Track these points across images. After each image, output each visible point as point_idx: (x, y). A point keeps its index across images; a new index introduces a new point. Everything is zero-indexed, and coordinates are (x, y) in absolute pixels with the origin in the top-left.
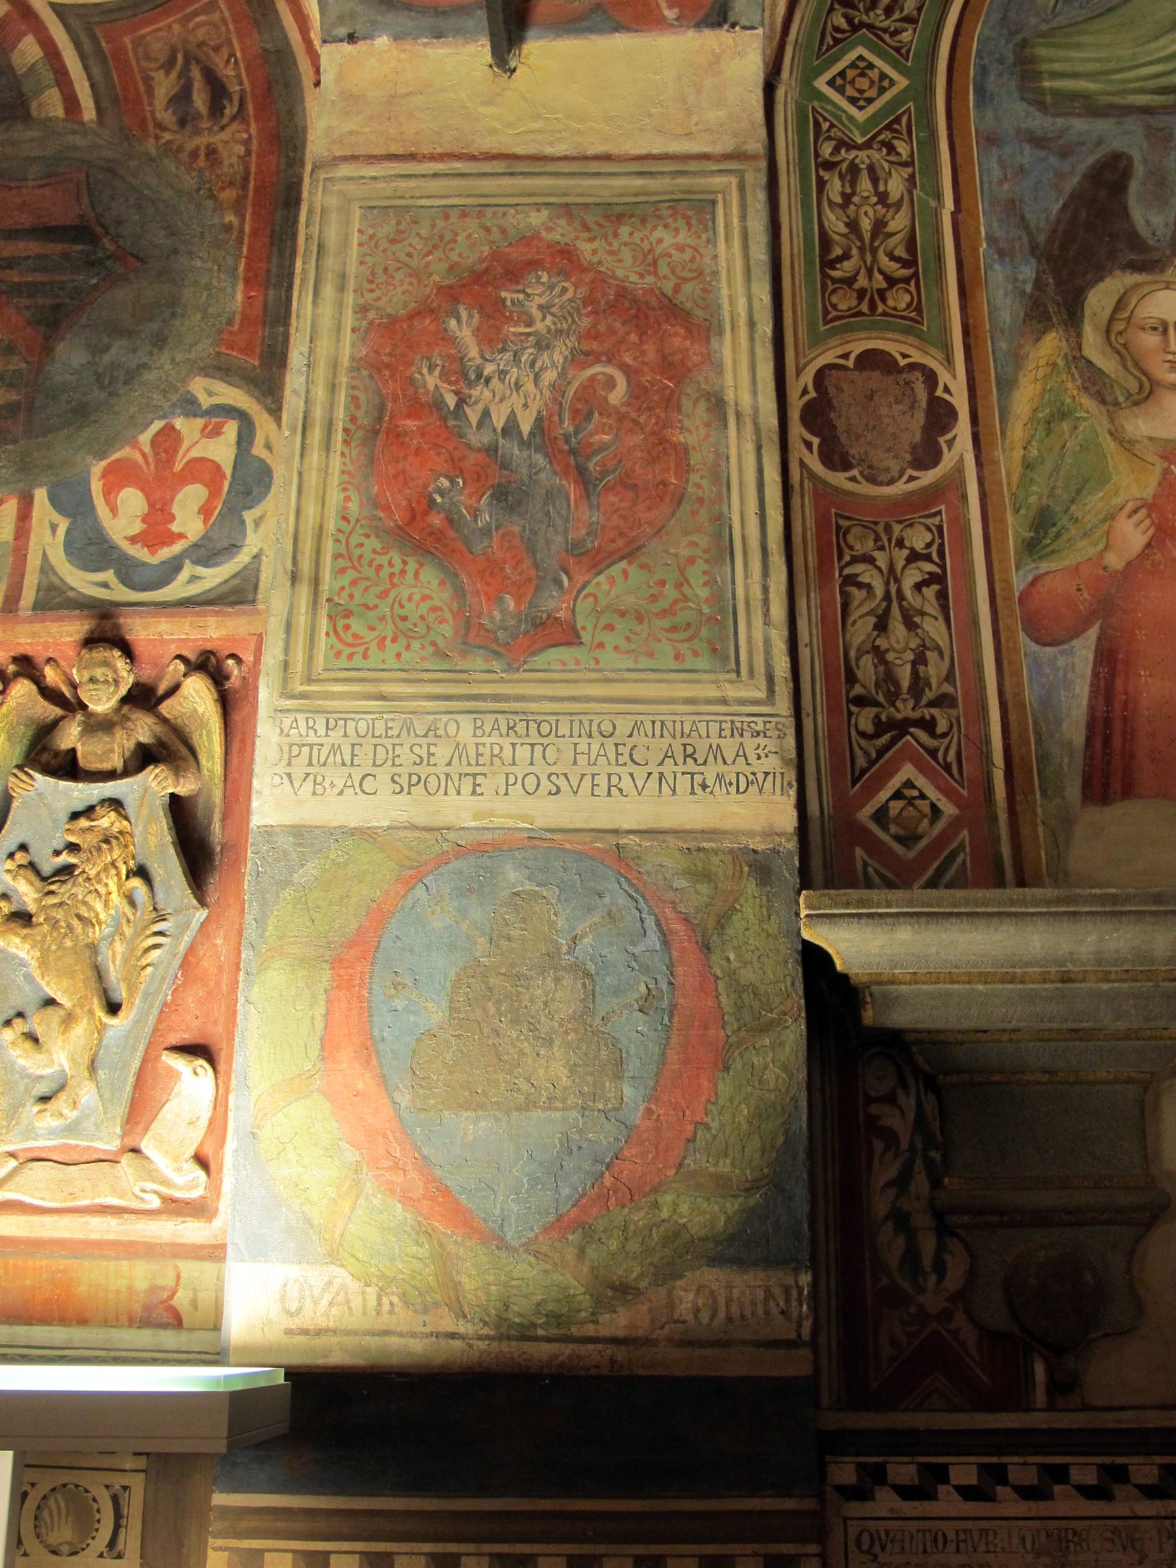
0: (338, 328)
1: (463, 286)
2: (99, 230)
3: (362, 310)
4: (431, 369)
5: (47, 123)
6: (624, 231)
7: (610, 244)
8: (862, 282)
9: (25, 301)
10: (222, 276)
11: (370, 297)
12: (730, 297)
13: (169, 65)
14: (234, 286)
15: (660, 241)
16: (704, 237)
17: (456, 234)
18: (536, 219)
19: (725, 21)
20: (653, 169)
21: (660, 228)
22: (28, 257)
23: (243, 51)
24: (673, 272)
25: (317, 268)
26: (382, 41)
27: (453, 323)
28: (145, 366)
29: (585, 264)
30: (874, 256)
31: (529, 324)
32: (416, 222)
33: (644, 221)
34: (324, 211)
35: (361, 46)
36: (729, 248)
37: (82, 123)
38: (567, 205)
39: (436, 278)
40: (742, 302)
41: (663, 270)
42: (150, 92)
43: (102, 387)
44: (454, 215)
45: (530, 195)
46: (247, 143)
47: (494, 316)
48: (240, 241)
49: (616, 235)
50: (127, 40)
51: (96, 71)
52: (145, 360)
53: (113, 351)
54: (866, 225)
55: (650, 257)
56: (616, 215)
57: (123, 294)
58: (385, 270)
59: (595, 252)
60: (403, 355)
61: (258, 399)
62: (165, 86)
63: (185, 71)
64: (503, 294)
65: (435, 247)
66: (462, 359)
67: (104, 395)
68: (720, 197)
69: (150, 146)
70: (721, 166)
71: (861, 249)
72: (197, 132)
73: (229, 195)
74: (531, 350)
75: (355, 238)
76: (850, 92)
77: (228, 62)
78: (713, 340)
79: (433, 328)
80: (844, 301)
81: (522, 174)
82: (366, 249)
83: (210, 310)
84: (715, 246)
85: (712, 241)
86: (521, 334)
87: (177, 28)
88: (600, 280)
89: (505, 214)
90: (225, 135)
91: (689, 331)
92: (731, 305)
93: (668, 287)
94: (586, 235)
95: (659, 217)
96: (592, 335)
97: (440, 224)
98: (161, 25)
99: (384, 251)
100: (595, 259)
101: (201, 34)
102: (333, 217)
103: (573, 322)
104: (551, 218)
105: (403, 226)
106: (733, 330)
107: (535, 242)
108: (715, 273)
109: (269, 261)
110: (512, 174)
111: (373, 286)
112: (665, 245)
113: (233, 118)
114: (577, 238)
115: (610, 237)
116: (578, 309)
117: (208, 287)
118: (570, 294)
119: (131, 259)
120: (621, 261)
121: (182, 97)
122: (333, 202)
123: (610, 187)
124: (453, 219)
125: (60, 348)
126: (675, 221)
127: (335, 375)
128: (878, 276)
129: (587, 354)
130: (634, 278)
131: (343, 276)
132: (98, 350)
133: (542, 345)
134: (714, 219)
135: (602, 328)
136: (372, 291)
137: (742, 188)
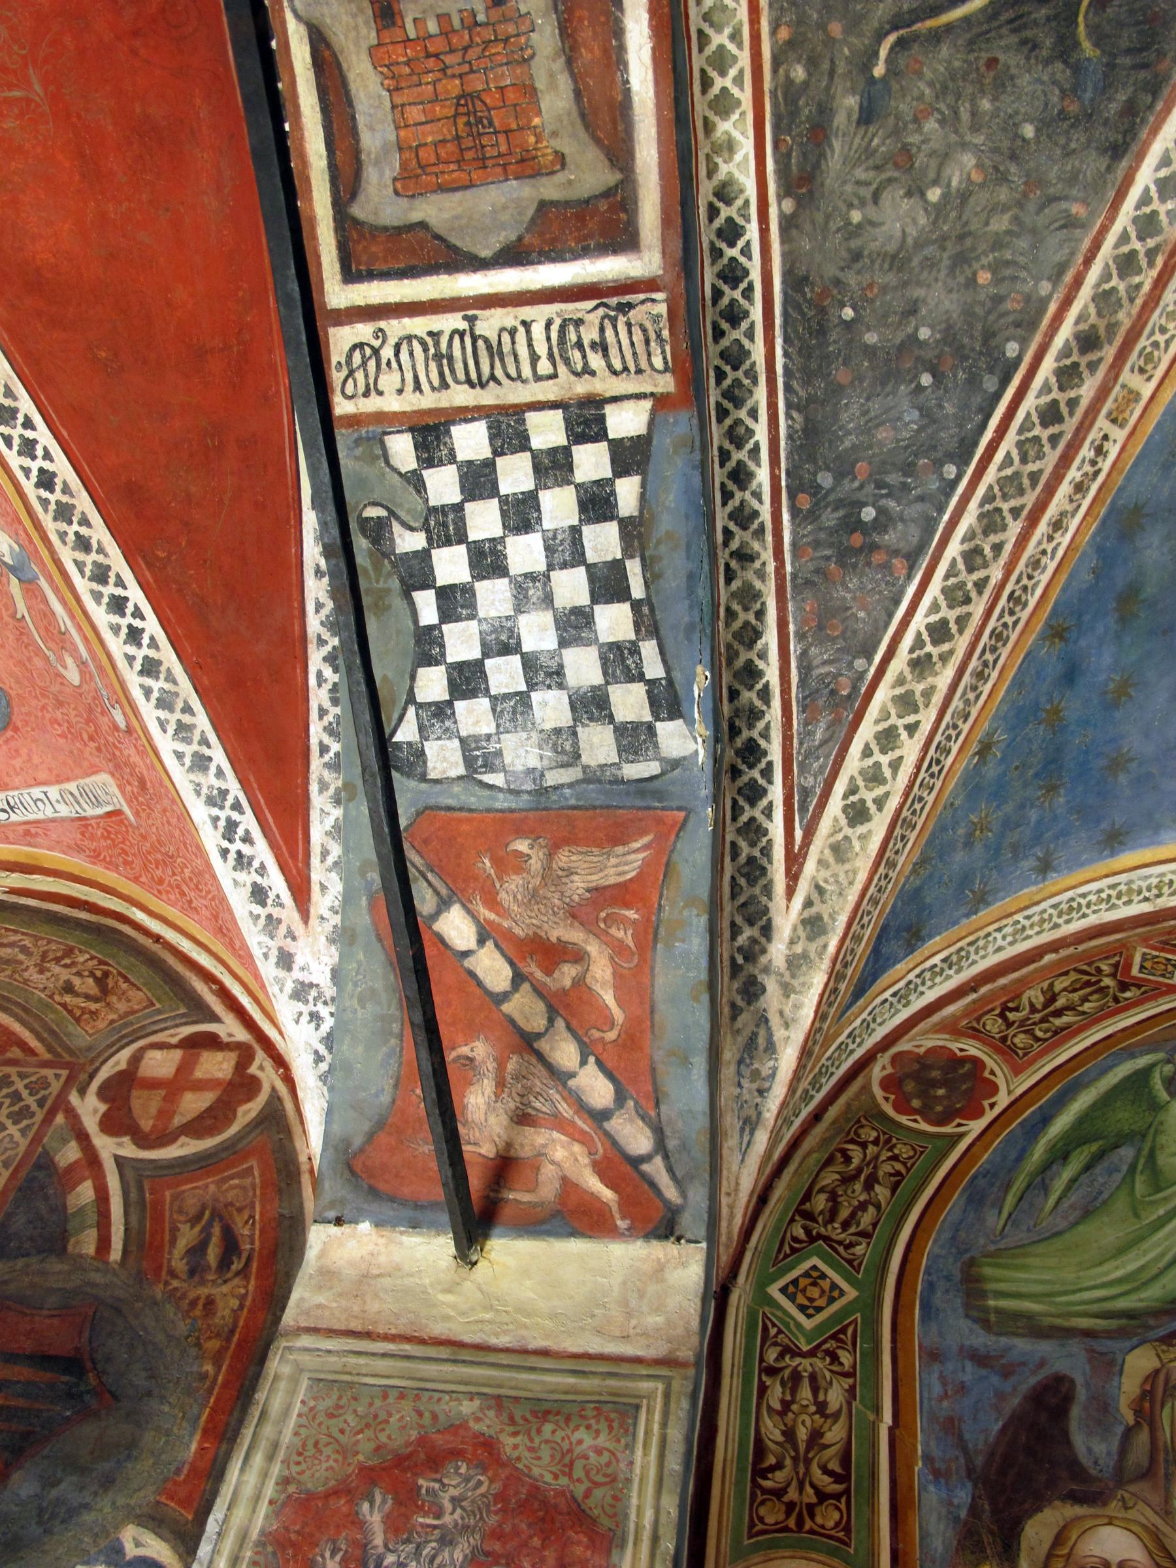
0: (257, 1498)
1: (384, 1469)
2: (89, 1364)
3: (285, 1481)
4: (333, 1554)
6: (548, 1428)
7: (531, 1440)
8: (792, 1494)
10: (185, 1424)
11: (295, 1469)
12: (639, 1507)
13: (195, 1220)
14: (192, 1435)
15: (580, 1442)
16: (623, 1441)
17: (390, 1415)
18: (468, 1407)
19: (672, 1234)
20: (586, 1369)
21: (582, 1429)
22: (18, 1382)
23: (261, 1214)
24: (587, 1473)
25: (254, 1434)
26: (365, 1227)
27: (366, 1506)
28: (86, 1507)
29: (504, 1457)
30: (807, 1469)
31: (438, 1516)
32: (356, 1399)
33: (568, 1419)
34: (276, 1378)
35: (346, 1229)
36: (645, 1454)
37: (107, 1263)
38: (498, 1398)
39: (361, 1457)
40: (649, 1515)
41: (578, 1472)
42: (173, 1242)
43: (40, 1523)
44: (393, 1394)
45: (466, 1384)
46: (243, 1298)
47: (407, 1501)
48: (210, 1391)
49: (539, 1431)
51: (134, 1219)
52: (88, 1500)
53: (63, 1486)
54: (802, 1434)
55: (567, 1460)
56: (544, 1411)
57: (89, 1430)
58: (316, 1444)
59: (515, 1447)
60: (311, 1535)
61: (180, 1556)
62: (187, 1237)
64: (421, 1482)
65: (368, 1426)
66: (366, 1545)
67: (41, 1530)
68: (645, 1401)
69: (158, 1291)
70: (651, 1372)
71: (795, 1460)
72: (203, 1282)
73: (213, 1345)
74: (434, 1544)
75: (297, 1407)
76: (801, 1299)
77: (247, 1222)
78: (614, 1551)
79: (344, 1509)
80: (772, 1514)
81: (464, 1362)
82: (304, 1421)
83: (164, 1457)
84: (633, 1452)
85: (631, 1447)
86: (429, 1526)
87: (212, 1188)
88: (516, 1477)
89: (439, 1400)
90: (225, 1289)
91: (591, 1539)
92: (638, 1516)
93: (579, 1490)
94: (512, 1429)
95: (583, 1417)
96: (497, 1534)
97: (378, 1403)
98: (200, 1183)
99: (320, 1424)
100: (516, 1454)
101: (230, 1196)
102: (282, 1385)
103: (481, 1518)
104: (481, 1409)
105: (343, 1402)
106: (635, 1544)
107: (462, 1432)
108: (628, 1481)
109: (231, 1414)
110: (455, 1361)
111: (301, 1459)
112: (585, 1445)
113: (237, 1274)
114: (502, 1431)
115: (533, 1433)
116: (488, 1506)
117: (168, 1433)
118: (483, 1489)
119: (107, 1395)
120: (539, 1458)
121: (197, 1250)
122: (286, 1370)
123: (543, 1383)
124: (391, 1400)
125: (16, 1476)
126: (598, 1422)
127: (241, 1546)
128: (809, 1490)
129: (487, 1554)
130: (548, 1478)
131: (275, 1445)
132: (49, 1482)
133: (446, 1540)
134: (635, 1424)
135: (507, 1528)
136: (298, 1463)
137: (667, 1396)
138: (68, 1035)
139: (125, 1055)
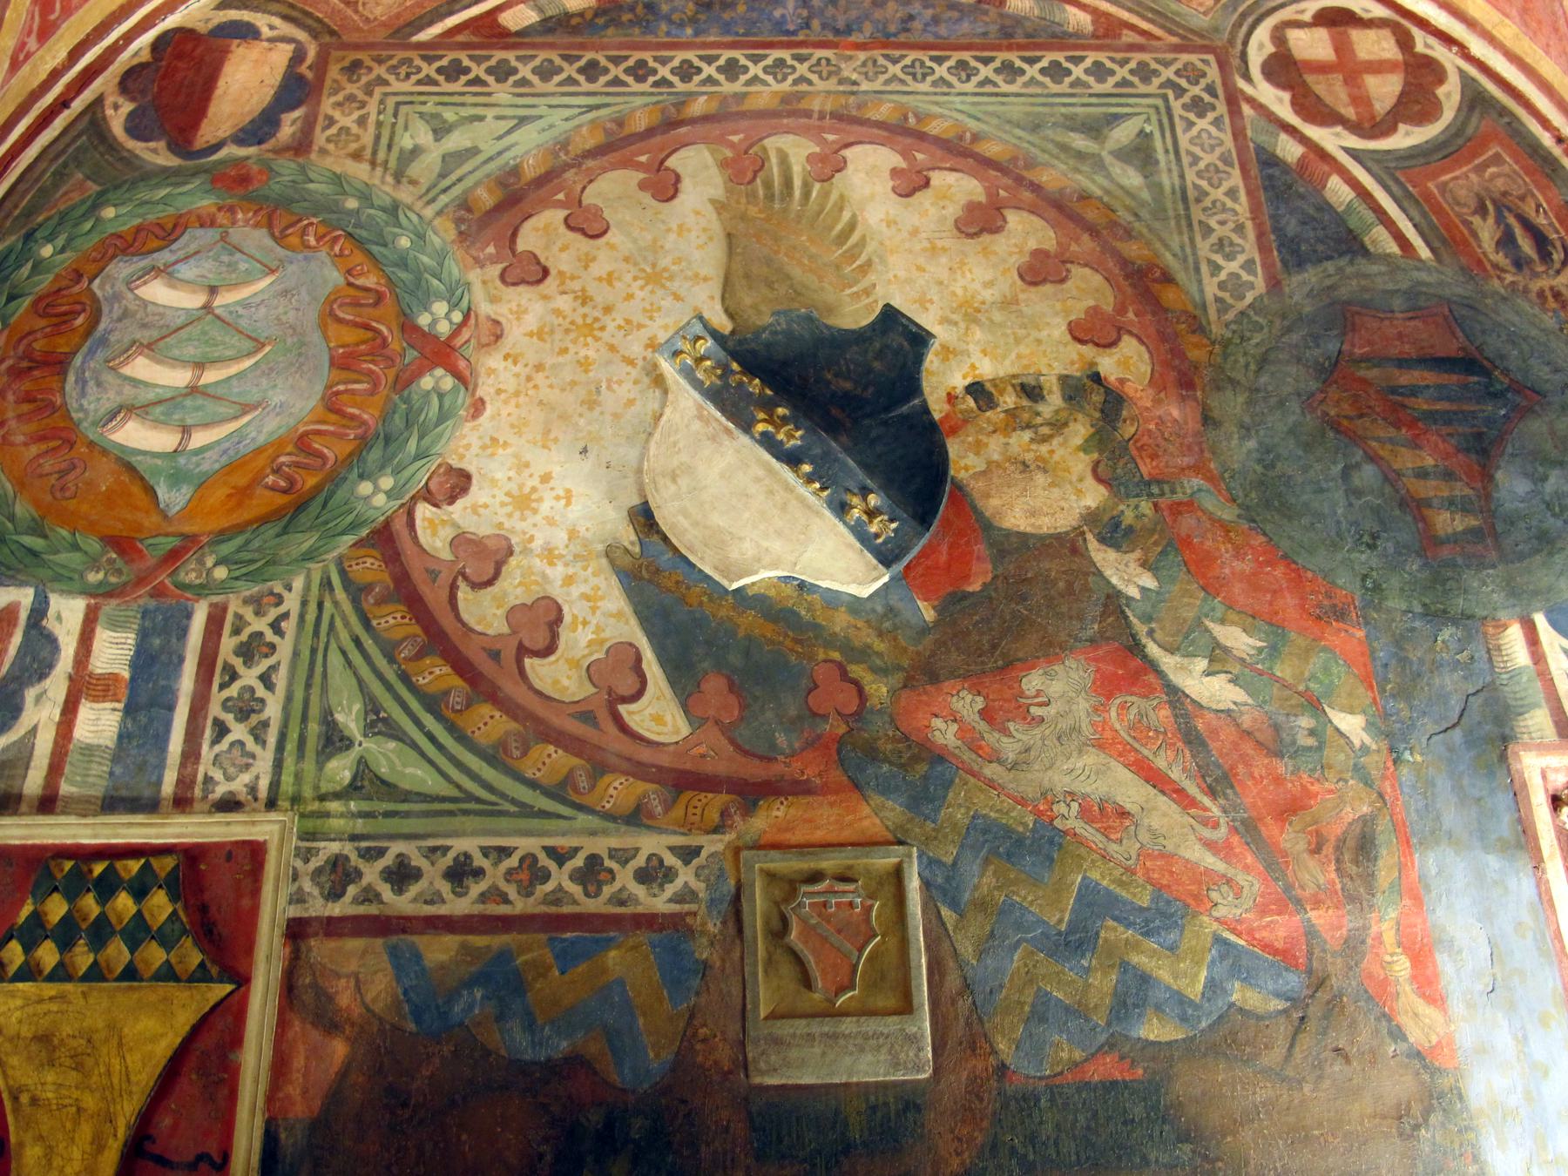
5: (1386, 258)
9: (1445, 430)
22: (1427, 386)
23: (1548, 203)
37: (1420, 260)
42: (1475, 234)
43: (1554, 515)
50: (1431, 185)
53: (1552, 480)
57: (1535, 426)
62: (1487, 232)
63: (1500, 219)
72: (1535, 275)
77: (1537, 211)
87: (1473, 177)
98: (1457, 173)
101: (1500, 184)
121: (1506, 241)
125: (1499, 475)
138: (1178, 14)
139: (1262, 34)
